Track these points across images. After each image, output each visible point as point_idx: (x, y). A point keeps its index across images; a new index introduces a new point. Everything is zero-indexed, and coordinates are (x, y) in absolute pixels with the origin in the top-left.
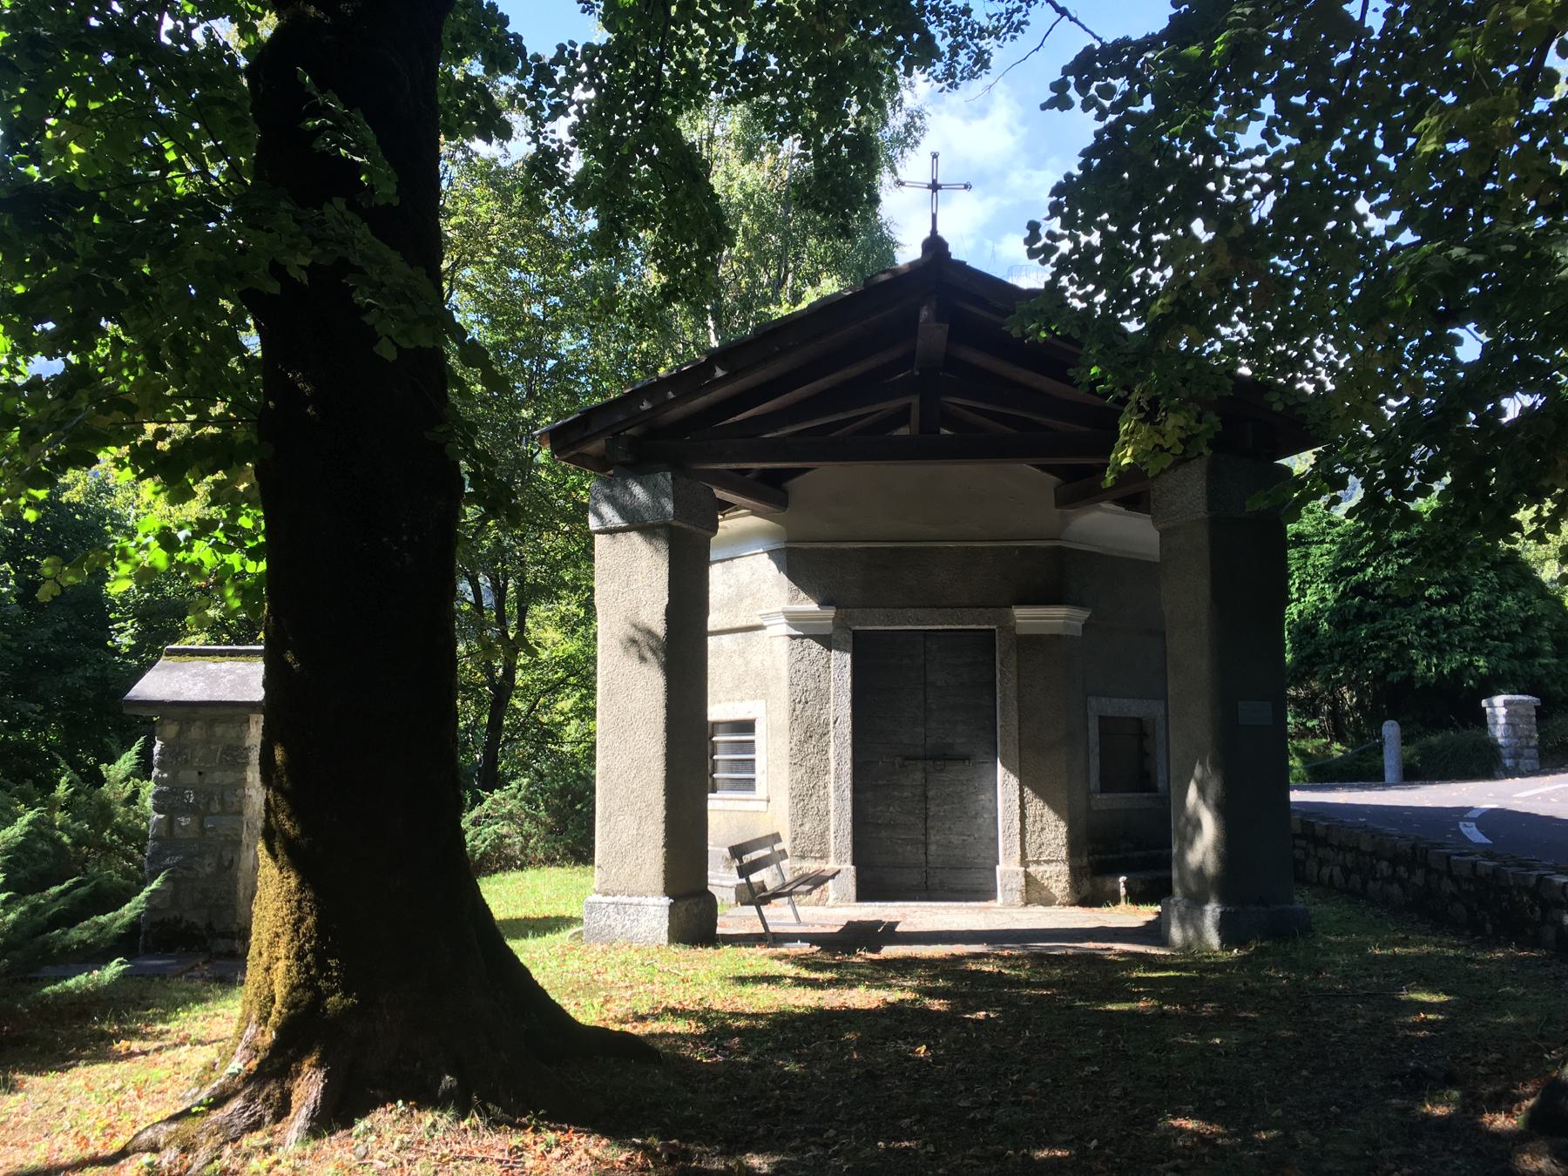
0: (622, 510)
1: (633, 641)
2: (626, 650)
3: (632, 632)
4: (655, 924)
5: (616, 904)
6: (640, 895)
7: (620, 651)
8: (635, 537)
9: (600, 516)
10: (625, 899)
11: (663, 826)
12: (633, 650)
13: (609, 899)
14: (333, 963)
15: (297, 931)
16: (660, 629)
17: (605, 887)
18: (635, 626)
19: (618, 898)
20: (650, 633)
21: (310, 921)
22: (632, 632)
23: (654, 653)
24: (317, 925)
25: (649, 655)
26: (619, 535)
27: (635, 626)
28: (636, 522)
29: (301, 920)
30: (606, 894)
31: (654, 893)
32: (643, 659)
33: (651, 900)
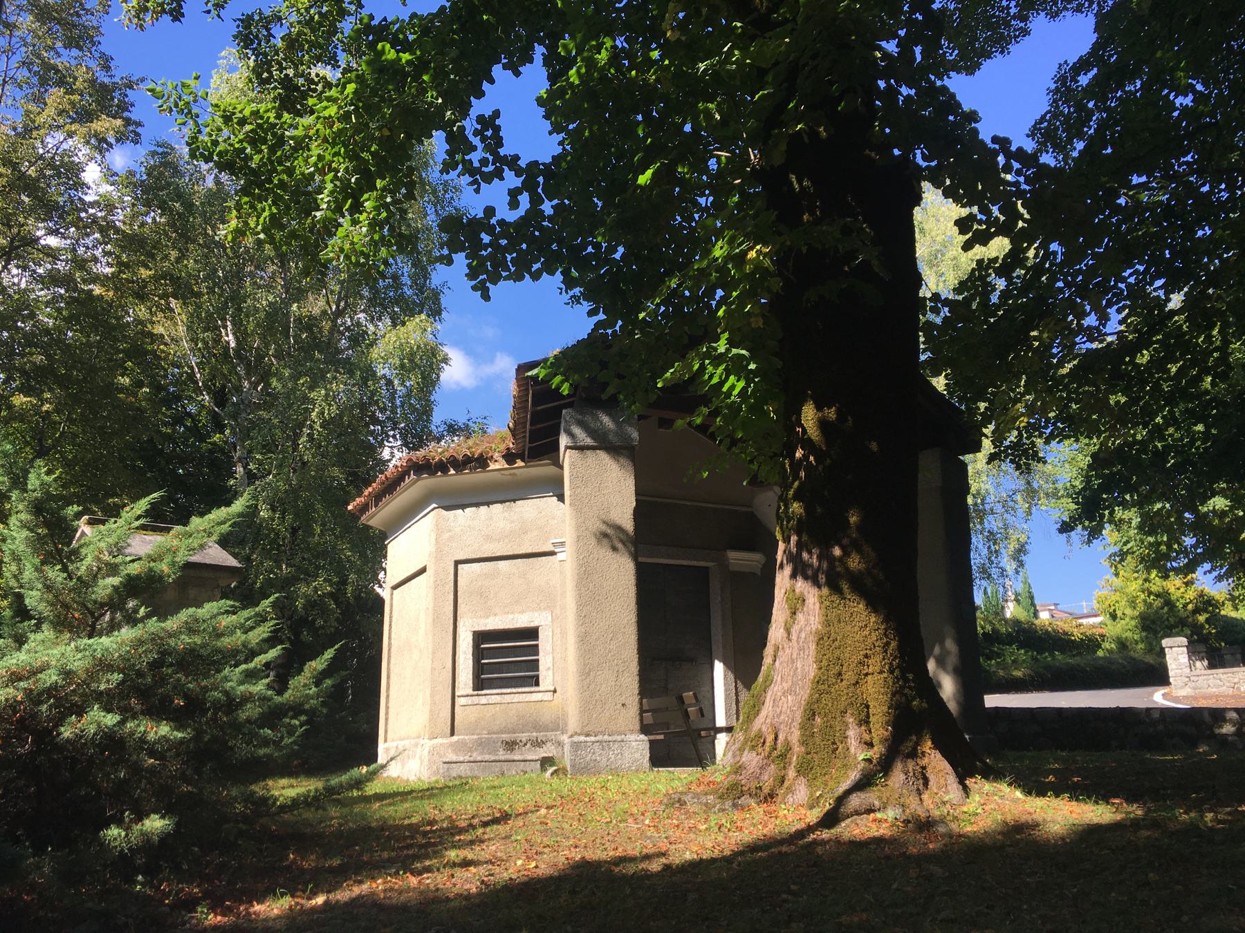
0: (591, 432)
1: (605, 535)
2: (599, 541)
3: (604, 528)
4: (637, 755)
5: (601, 742)
6: (620, 734)
7: (593, 541)
8: (602, 455)
9: (571, 435)
10: (606, 737)
11: (637, 678)
12: (605, 541)
13: (593, 739)
14: (911, 676)
15: (886, 652)
16: (628, 524)
17: (586, 729)
18: (604, 522)
19: (599, 738)
20: (619, 528)
21: (893, 644)
22: (604, 528)
23: (624, 543)
24: (900, 647)
25: (620, 546)
26: (589, 452)
27: (604, 522)
28: (604, 443)
29: (888, 644)
30: (587, 735)
31: (632, 731)
32: (614, 549)
33: (633, 737)
